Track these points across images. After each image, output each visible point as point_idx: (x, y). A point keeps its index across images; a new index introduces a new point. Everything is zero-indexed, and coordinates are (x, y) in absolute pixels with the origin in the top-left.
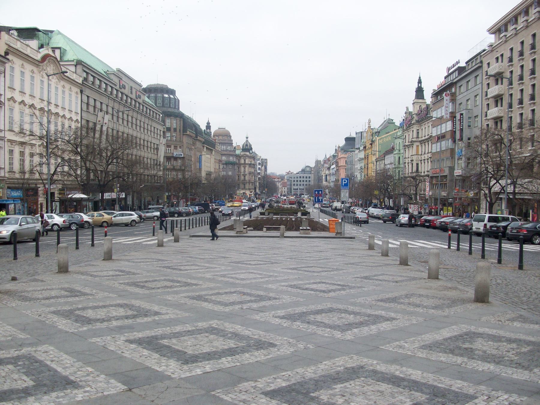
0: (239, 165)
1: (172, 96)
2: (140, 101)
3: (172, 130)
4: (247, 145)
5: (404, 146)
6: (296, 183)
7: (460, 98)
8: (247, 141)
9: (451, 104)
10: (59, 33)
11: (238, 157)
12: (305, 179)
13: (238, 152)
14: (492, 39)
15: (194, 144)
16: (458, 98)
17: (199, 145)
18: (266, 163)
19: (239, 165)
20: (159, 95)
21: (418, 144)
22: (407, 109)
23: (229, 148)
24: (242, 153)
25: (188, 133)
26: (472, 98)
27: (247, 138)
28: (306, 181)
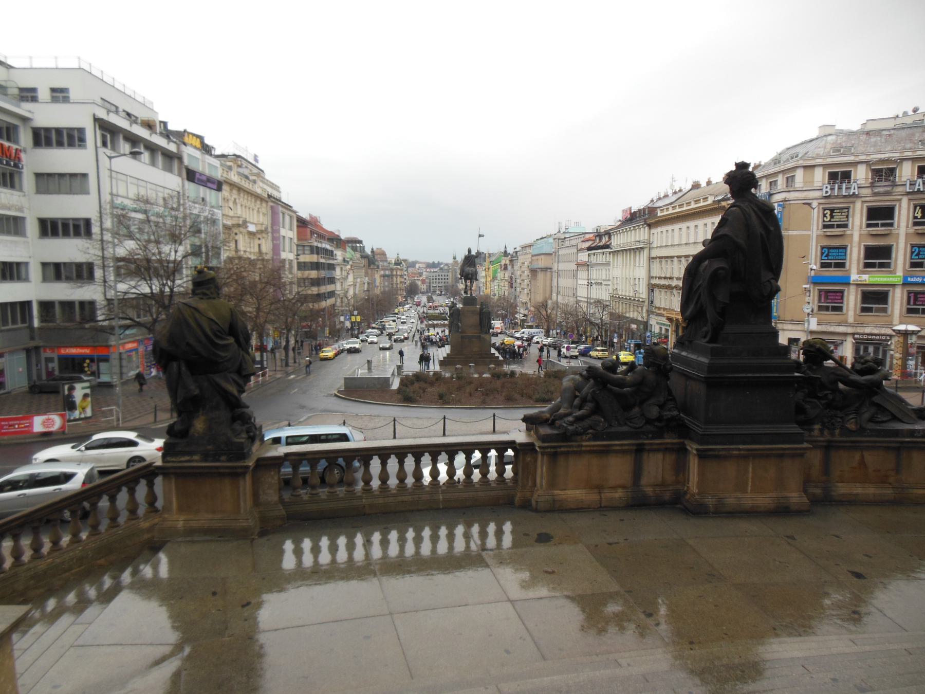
0: (392, 275)
4: (398, 260)
6: (435, 281)
11: (392, 270)
12: (443, 277)
13: (391, 266)
16: (515, 267)
19: (392, 275)
20: (354, 245)
23: (385, 264)
24: (395, 267)
28: (445, 279)
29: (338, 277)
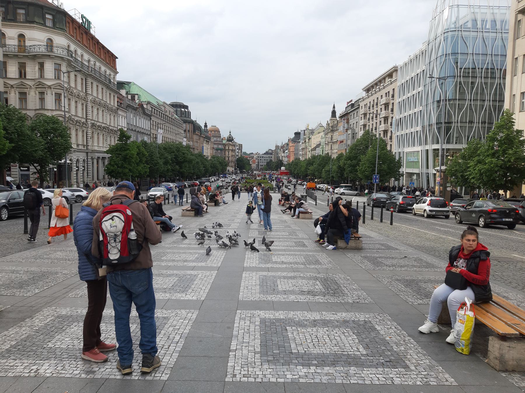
0: (225, 150)
1: (186, 110)
2: (173, 118)
3: (187, 131)
5: (325, 144)
7: (351, 122)
8: (230, 134)
9: (346, 124)
10: (134, 84)
11: (225, 145)
13: (224, 142)
14: (364, 94)
15: (199, 139)
16: (350, 121)
17: (202, 139)
18: (242, 147)
19: (225, 150)
20: (179, 109)
21: (331, 143)
22: (328, 122)
23: (218, 139)
25: (197, 133)
26: (355, 123)
27: (230, 132)
29: (49, 83)
